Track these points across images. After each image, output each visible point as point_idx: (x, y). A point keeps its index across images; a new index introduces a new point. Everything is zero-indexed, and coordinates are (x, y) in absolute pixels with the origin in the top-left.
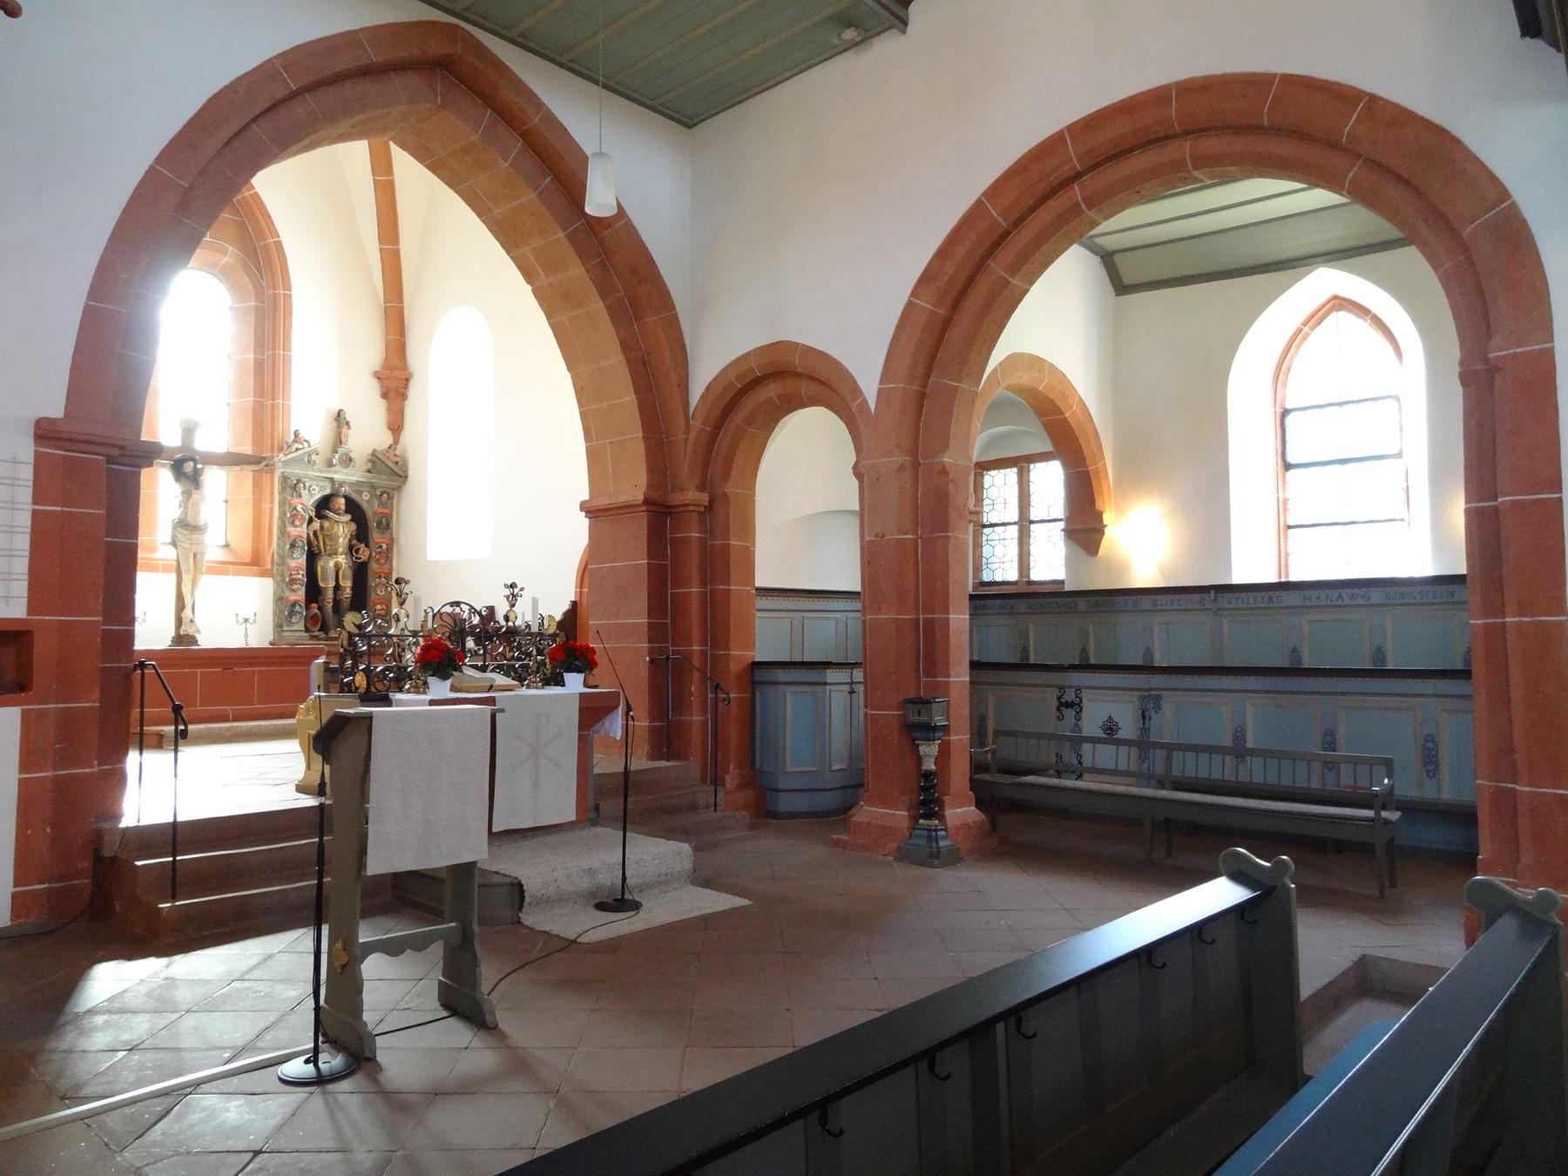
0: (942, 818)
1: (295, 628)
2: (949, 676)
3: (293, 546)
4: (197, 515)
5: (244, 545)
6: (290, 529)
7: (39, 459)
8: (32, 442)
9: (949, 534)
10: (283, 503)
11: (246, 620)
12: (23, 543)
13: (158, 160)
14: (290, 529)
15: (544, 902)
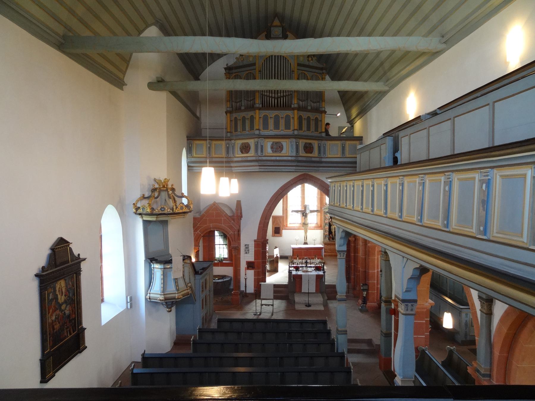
0: (366, 304)
1: (327, 239)
2: (369, 281)
3: (326, 224)
4: (306, 222)
5: (319, 223)
6: (325, 221)
7: (255, 244)
8: (254, 242)
9: (370, 257)
10: (324, 216)
11: (314, 240)
12: (253, 253)
13: (266, 207)
14: (325, 221)
15: (298, 303)
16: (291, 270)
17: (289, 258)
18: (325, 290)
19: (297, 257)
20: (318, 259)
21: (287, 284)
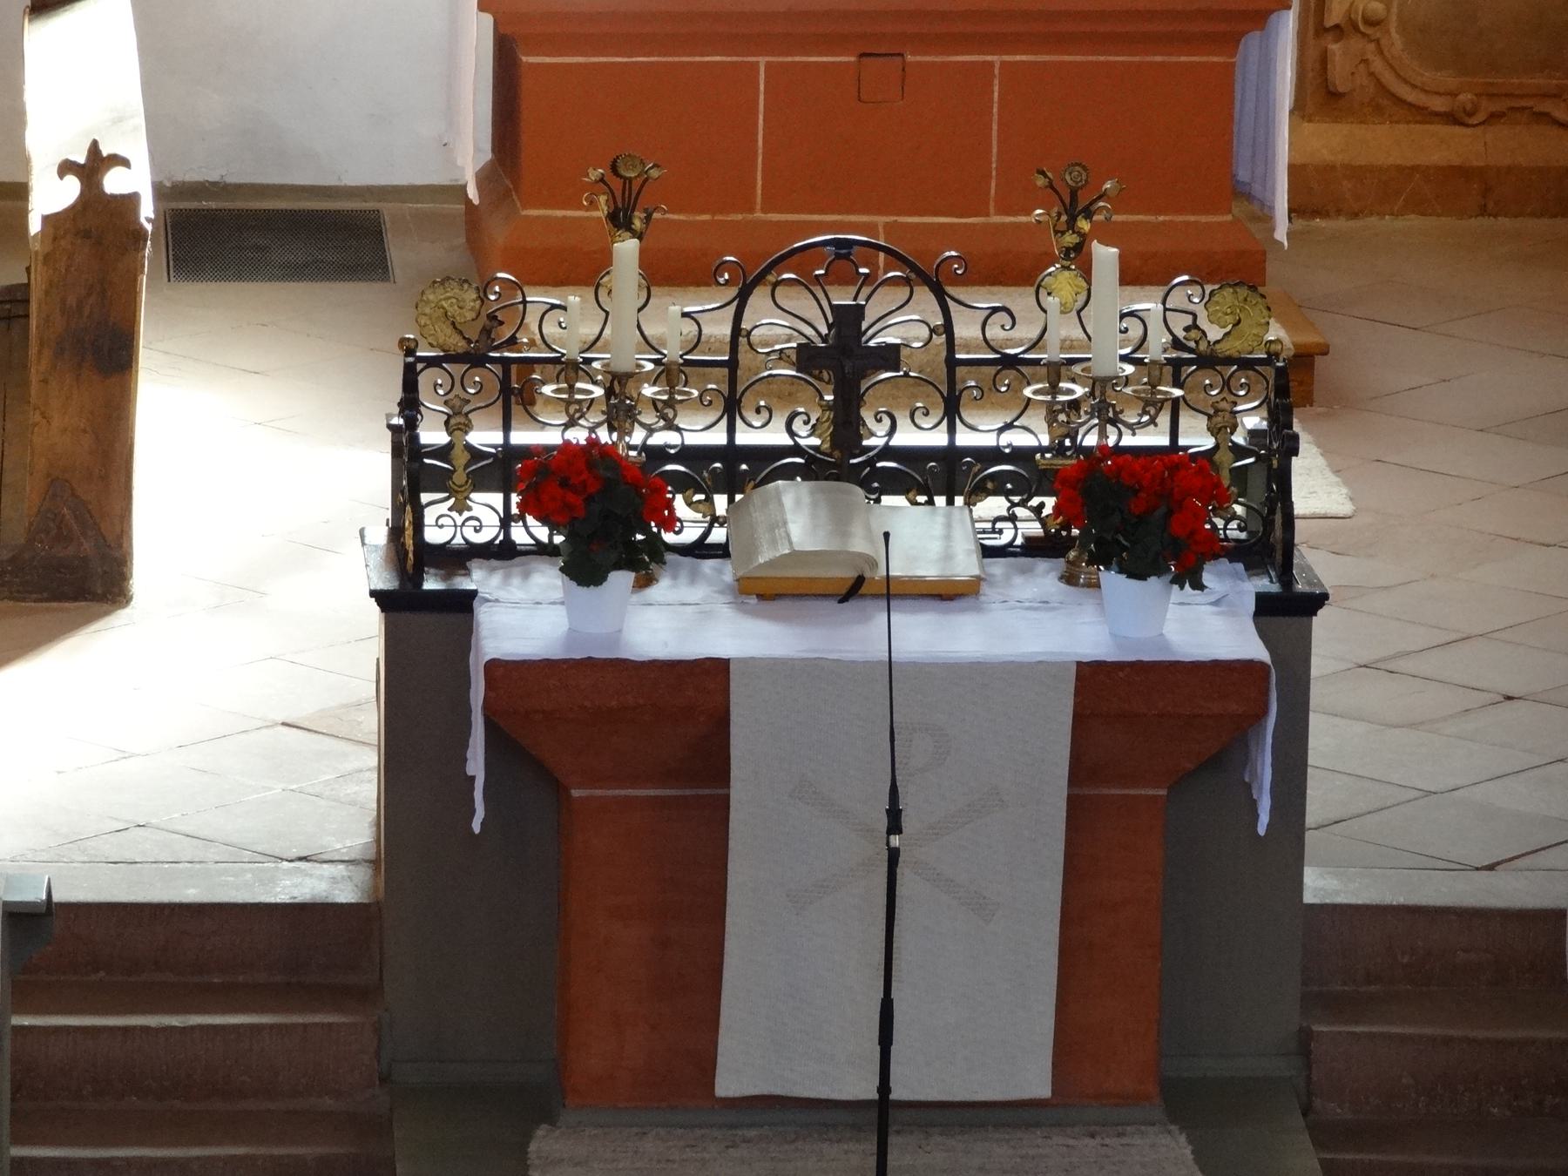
16: (456, 558)
17: (399, 253)
18: (1305, 1039)
19: (620, 220)
20: (1131, 276)
21: (346, 895)
